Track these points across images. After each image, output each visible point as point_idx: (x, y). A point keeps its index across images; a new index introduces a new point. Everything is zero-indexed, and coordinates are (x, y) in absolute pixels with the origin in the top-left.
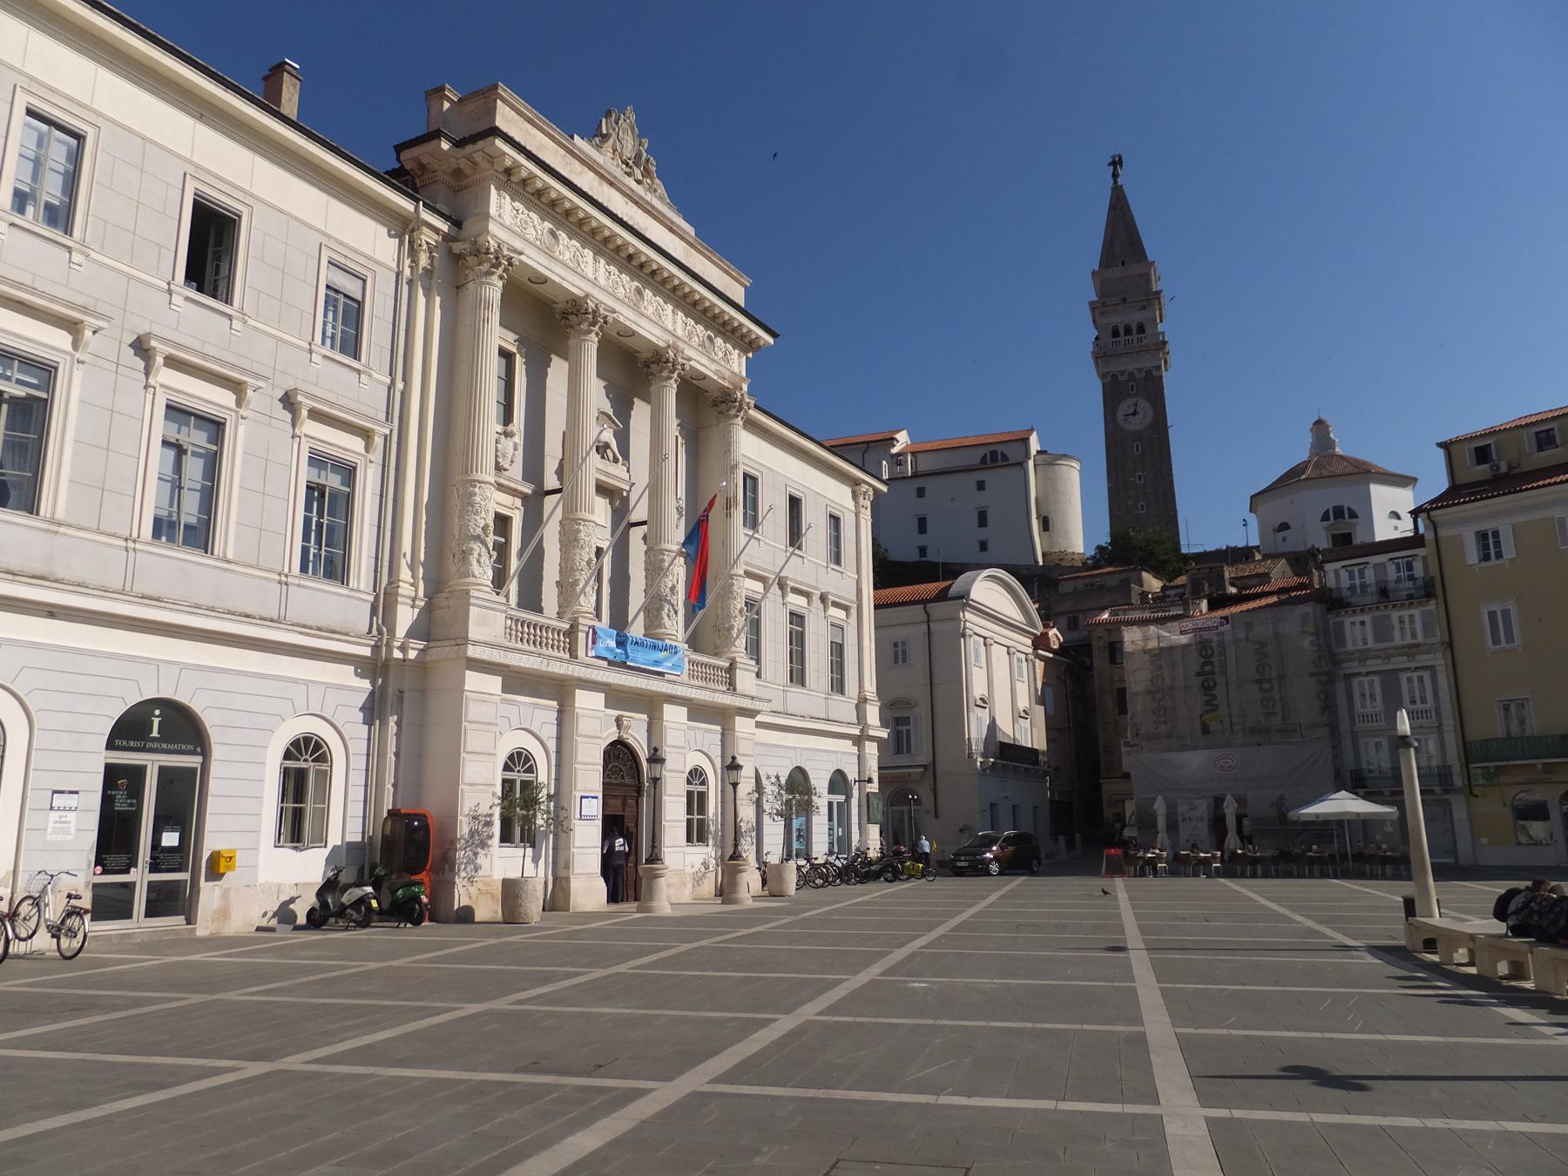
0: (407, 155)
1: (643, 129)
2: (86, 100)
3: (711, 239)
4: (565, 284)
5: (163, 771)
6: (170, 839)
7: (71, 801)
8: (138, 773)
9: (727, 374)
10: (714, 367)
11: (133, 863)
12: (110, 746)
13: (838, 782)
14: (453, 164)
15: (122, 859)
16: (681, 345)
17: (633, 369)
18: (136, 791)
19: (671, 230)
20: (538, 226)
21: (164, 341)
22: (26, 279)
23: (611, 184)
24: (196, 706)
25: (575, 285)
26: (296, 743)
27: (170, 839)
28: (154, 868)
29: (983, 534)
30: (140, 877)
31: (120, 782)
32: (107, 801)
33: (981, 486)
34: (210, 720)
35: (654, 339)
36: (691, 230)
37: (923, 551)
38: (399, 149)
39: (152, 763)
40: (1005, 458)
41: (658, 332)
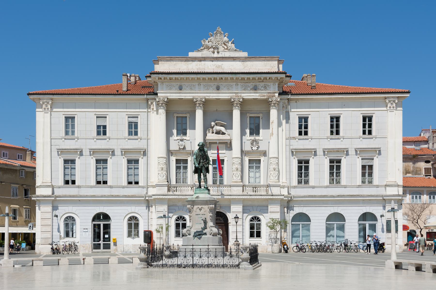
4: (187, 97)
5: (104, 225)
6: (107, 236)
7: (86, 230)
8: (99, 225)
9: (265, 94)
11: (100, 240)
14: (153, 82)
15: (98, 239)
18: (99, 228)
26: (130, 218)
27: (107, 236)
28: (104, 241)
30: (101, 242)
31: (96, 228)
32: (94, 231)
35: (227, 97)
36: (245, 54)
39: (102, 223)
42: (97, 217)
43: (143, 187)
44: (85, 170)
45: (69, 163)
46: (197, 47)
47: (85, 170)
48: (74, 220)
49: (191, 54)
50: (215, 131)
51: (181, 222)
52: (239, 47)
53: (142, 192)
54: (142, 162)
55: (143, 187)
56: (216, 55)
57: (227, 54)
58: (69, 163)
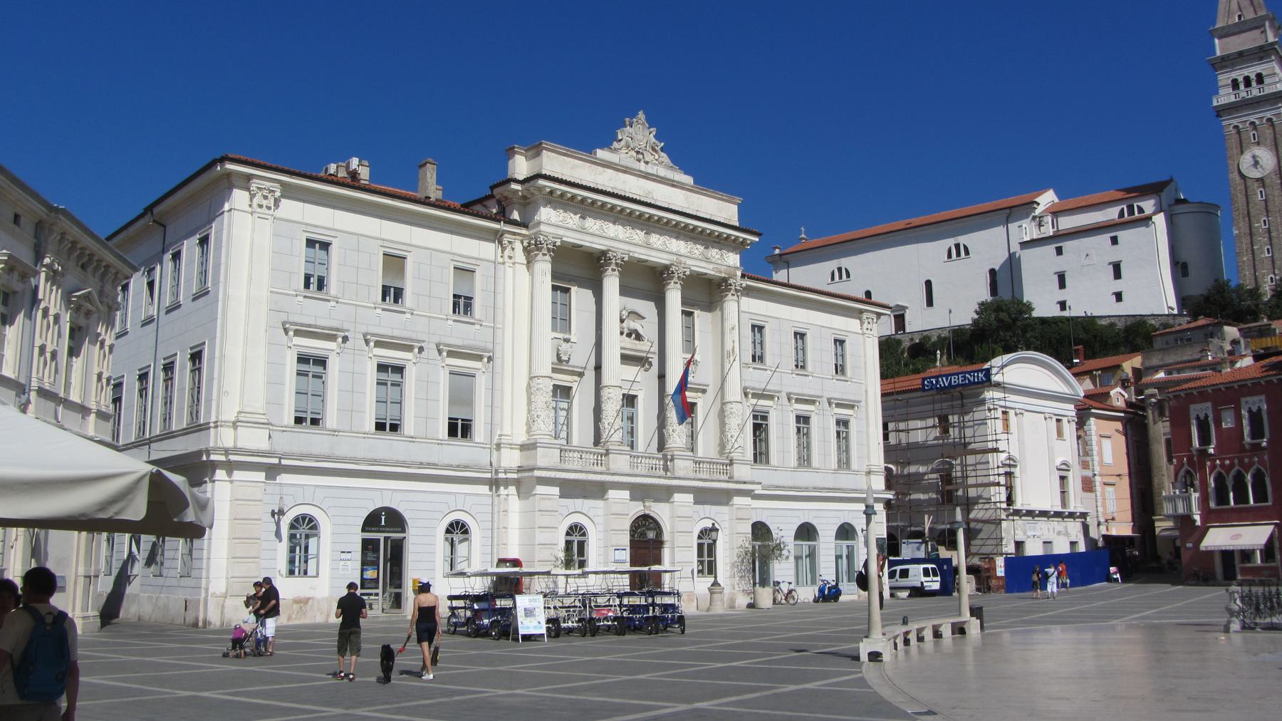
0: (496, 191)
1: (651, 122)
2: (330, 225)
3: (707, 182)
7: (348, 556)
9: (723, 268)
10: (711, 266)
12: (363, 530)
13: (845, 532)
16: (683, 259)
17: (648, 281)
18: (377, 550)
19: (673, 186)
20: (573, 220)
21: (373, 335)
22: (312, 322)
23: (625, 172)
24: (401, 510)
25: (598, 245)
26: (451, 525)
29: (1118, 286)
33: (1114, 241)
34: (406, 515)
36: (688, 180)
37: (1063, 305)
38: (492, 188)
39: (381, 536)
40: (1141, 210)
41: (665, 256)
42: (372, 522)
43: (481, 446)
44: (351, 387)
45: (312, 364)
46: (607, 140)
47: (351, 387)
48: (315, 527)
49: (601, 154)
50: (626, 331)
51: (576, 539)
52: (680, 160)
53: (483, 457)
54: (481, 383)
55: (481, 446)
56: (642, 166)
57: (662, 172)
58: (312, 364)
